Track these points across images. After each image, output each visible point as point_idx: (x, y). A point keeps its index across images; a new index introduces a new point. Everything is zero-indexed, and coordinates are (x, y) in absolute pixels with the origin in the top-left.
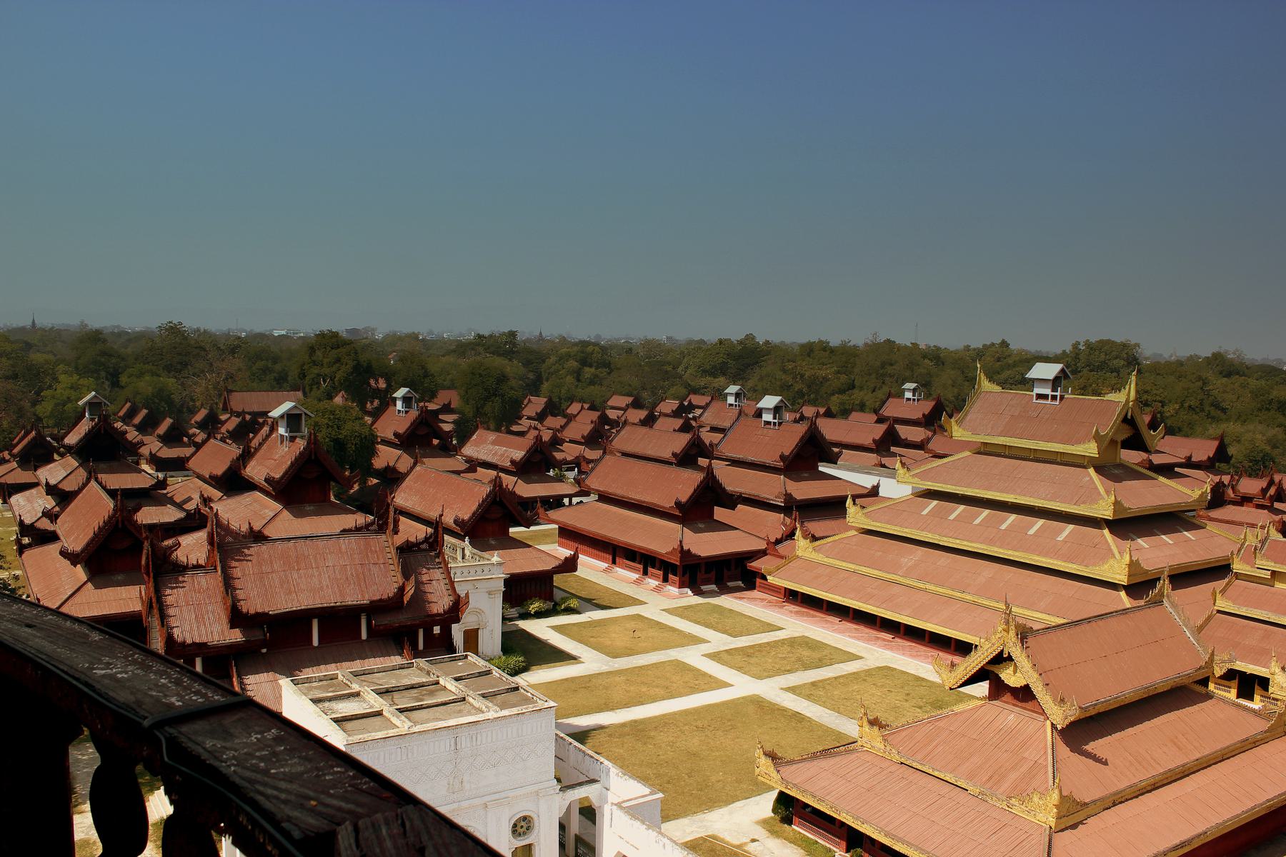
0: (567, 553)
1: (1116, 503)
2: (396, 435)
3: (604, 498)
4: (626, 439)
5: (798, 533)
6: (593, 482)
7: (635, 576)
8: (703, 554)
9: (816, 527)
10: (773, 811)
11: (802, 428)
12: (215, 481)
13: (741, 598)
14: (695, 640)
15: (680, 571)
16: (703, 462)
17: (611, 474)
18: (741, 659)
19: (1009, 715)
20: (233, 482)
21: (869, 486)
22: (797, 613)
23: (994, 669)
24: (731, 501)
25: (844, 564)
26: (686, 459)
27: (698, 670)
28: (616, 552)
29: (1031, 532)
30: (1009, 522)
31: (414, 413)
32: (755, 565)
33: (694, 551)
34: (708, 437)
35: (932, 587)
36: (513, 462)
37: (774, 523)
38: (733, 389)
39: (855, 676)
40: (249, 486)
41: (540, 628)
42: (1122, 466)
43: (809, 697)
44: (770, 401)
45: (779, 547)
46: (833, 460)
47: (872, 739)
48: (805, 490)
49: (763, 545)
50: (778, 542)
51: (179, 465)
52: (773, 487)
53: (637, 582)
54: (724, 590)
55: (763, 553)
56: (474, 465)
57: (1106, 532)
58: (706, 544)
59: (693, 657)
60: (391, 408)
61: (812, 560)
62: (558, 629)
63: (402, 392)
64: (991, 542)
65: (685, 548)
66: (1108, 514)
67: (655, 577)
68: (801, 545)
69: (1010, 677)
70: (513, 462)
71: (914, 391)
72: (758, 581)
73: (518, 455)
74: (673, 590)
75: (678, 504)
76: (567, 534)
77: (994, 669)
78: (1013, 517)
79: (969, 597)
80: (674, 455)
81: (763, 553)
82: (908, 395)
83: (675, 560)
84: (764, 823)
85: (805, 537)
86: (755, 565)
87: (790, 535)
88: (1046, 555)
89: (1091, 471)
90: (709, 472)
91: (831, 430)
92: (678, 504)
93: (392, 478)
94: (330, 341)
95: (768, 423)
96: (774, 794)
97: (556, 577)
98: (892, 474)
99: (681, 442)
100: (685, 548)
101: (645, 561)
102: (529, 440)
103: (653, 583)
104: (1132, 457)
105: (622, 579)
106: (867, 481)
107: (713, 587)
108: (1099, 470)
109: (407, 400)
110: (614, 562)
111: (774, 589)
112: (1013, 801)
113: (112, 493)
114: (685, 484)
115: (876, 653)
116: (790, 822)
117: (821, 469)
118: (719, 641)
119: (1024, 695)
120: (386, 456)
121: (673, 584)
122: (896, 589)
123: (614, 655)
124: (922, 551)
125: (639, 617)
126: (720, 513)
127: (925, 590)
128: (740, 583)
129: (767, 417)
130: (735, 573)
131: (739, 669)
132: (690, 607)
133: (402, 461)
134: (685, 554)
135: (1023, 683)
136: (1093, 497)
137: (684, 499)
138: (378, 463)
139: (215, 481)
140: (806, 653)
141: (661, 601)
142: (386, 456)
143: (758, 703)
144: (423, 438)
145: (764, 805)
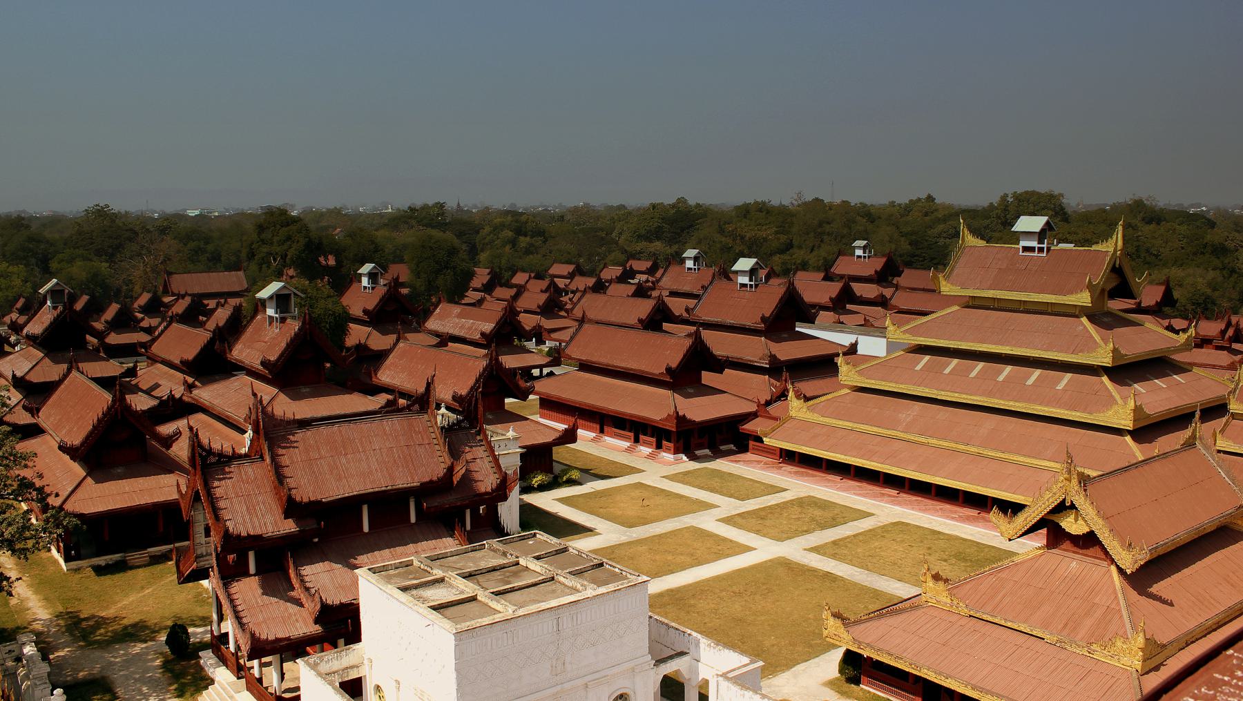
0: (562, 427)
1: (1115, 351)
3: (585, 367)
5: (791, 394)
6: (575, 352)
7: (626, 444)
8: (698, 419)
9: (808, 387)
10: (840, 671)
13: (736, 462)
14: (708, 506)
15: (674, 437)
18: (758, 521)
19: (1071, 563)
21: (847, 344)
22: (796, 473)
23: (1055, 518)
25: (841, 422)
26: (657, 320)
27: (717, 536)
28: (606, 421)
31: (381, 290)
32: (749, 427)
33: (688, 417)
36: (483, 334)
37: (762, 386)
38: (691, 253)
39: (872, 533)
41: (547, 501)
42: (1110, 314)
43: (834, 556)
45: (769, 408)
46: (810, 320)
47: (937, 594)
49: (753, 408)
50: (768, 403)
52: (756, 349)
54: (718, 454)
55: (754, 415)
56: (444, 340)
58: (700, 409)
59: (707, 522)
60: (355, 285)
61: (804, 419)
62: (563, 500)
64: (990, 394)
65: (681, 414)
68: (795, 406)
69: (1071, 525)
70: (483, 334)
71: (864, 248)
72: (751, 443)
73: (488, 327)
74: (668, 456)
77: (1055, 518)
78: (1008, 369)
80: (640, 321)
81: (754, 415)
82: (859, 252)
84: (831, 684)
85: (798, 397)
86: (749, 427)
89: (1084, 320)
96: (838, 654)
97: (554, 449)
98: (868, 327)
99: (644, 308)
101: (636, 429)
103: (646, 450)
104: (1116, 305)
106: (845, 339)
107: (707, 451)
108: (1092, 319)
110: (602, 431)
111: (769, 451)
115: (887, 510)
116: (856, 681)
118: (729, 506)
119: (1089, 541)
120: (357, 334)
121: (668, 450)
122: (897, 445)
123: (629, 524)
125: (640, 485)
127: (927, 445)
128: (732, 446)
130: (727, 437)
131: (758, 532)
132: (689, 472)
133: (378, 341)
135: (1086, 530)
136: (1091, 346)
140: (818, 513)
141: (660, 469)
143: (785, 564)
145: (830, 664)
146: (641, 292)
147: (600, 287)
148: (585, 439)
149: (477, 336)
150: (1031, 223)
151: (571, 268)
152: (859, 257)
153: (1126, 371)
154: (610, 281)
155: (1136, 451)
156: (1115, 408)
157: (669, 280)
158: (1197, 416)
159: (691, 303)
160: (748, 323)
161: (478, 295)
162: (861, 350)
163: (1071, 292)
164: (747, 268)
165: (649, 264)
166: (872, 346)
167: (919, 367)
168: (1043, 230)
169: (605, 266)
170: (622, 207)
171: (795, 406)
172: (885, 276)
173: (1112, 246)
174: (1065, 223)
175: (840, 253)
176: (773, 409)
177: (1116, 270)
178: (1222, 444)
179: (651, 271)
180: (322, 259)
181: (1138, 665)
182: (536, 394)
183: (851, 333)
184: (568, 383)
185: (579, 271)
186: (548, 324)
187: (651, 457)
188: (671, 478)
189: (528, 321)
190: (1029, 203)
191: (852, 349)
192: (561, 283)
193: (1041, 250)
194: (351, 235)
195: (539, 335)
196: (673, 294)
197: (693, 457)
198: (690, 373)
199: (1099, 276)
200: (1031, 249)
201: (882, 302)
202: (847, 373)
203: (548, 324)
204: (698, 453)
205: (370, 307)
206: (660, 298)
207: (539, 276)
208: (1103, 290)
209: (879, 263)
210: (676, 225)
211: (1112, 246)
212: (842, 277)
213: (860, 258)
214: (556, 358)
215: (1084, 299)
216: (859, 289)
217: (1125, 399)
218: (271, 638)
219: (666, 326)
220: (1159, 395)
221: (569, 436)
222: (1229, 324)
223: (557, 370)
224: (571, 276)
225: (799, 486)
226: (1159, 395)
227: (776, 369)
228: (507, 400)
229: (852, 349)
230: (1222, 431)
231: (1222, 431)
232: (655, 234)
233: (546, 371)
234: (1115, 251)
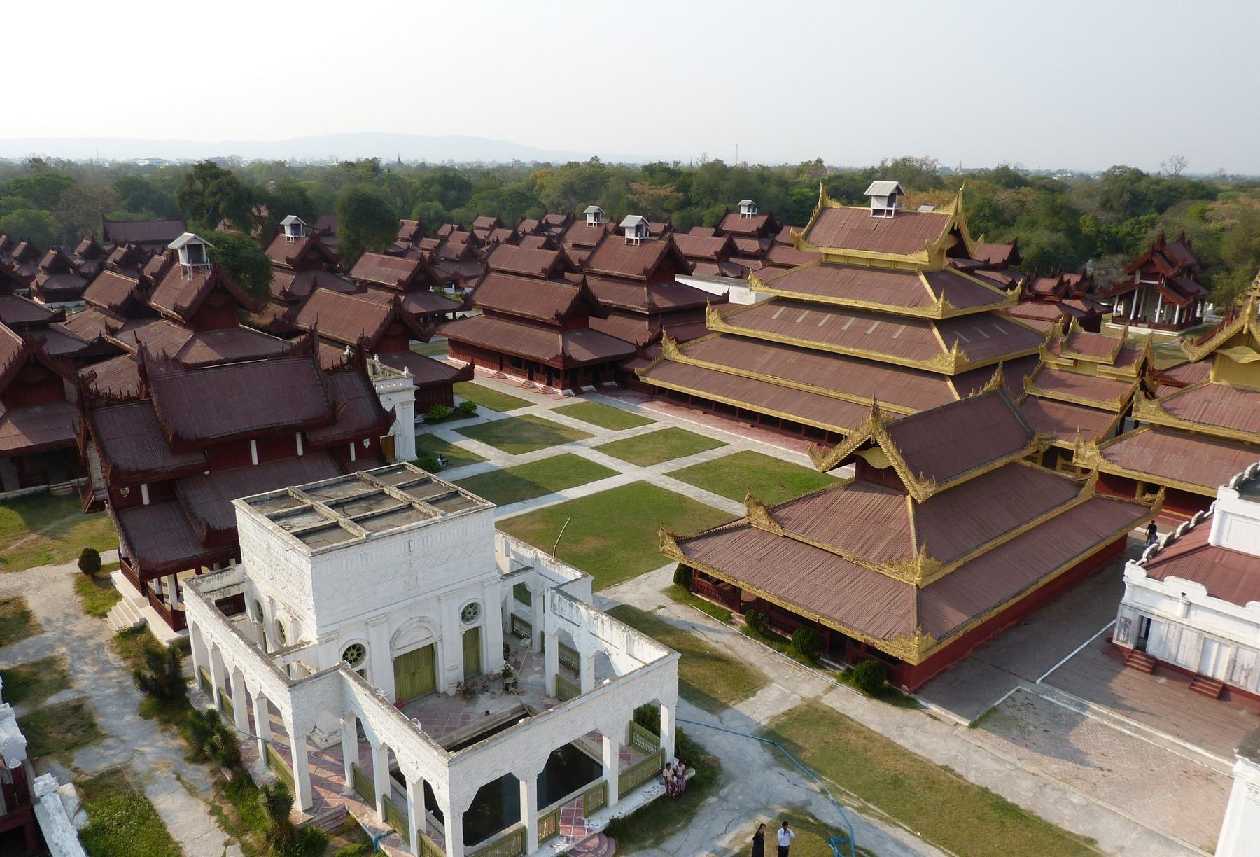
2: (288, 260)
3: (488, 312)
4: (503, 258)
6: (479, 300)
7: (522, 380)
11: (663, 244)
12: (115, 311)
16: (577, 277)
17: (494, 293)
20: (136, 310)
24: (604, 311)
26: (558, 271)
29: (870, 332)
32: (628, 366)
34: (575, 256)
35: (783, 382)
36: (400, 282)
40: (155, 315)
44: (631, 221)
49: (632, 350)
50: (646, 346)
51: (75, 294)
52: (638, 299)
53: (524, 385)
57: (935, 331)
63: (291, 218)
64: (834, 341)
67: (541, 381)
70: (400, 282)
73: (405, 275)
75: (558, 315)
76: (458, 347)
79: (816, 390)
86: (628, 366)
87: (656, 340)
88: (882, 352)
90: (584, 284)
91: (688, 244)
92: (558, 315)
93: (294, 301)
94: (209, 172)
95: (630, 241)
102: (412, 262)
105: (513, 384)
107: (591, 387)
109: (295, 227)
112: (884, 565)
113: (17, 328)
114: (563, 295)
118: (603, 435)
122: (753, 385)
124: (773, 350)
126: (594, 322)
128: (614, 383)
129: (630, 235)
134: (566, 358)
137: (563, 311)
138: (275, 290)
139: (115, 311)
140: (675, 442)
141: (545, 404)
142: (282, 281)
144: (318, 262)
146: (548, 245)
147: (515, 239)
148: (483, 374)
149: (395, 284)
151: (492, 220)
152: (744, 215)
154: (525, 234)
157: (572, 237)
160: (632, 275)
161: (404, 245)
162: (733, 299)
165: (563, 218)
166: (741, 295)
167: (775, 317)
169: (523, 220)
170: (548, 165)
172: (768, 232)
175: (728, 212)
176: (651, 352)
177: (955, 232)
180: (254, 210)
182: (444, 335)
184: (472, 324)
185: (499, 224)
186: (464, 271)
187: (543, 392)
188: (557, 410)
189: (443, 272)
191: (725, 298)
192: (480, 235)
194: (282, 188)
195: (456, 281)
196: (575, 246)
197: (579, 393)
199: (942, 239)
201: (761, 256)
203: (464, 271)
204: (584, 388)
205: (293, 255)
206: (562, 251)
207: (461, 229)
208: (941, 251)
209: (761, 221)
212: (728, 232)
213: (745, 216)
214: (468, 304)
216: (742, 244)
218: (161, 561)
219: (567, 275)
221: (467, 374)
223: (468, 314)
224: (492, 228)
227: (655, 315)
228: (412, 342)
229: (725, 298)
233: (458, 314)
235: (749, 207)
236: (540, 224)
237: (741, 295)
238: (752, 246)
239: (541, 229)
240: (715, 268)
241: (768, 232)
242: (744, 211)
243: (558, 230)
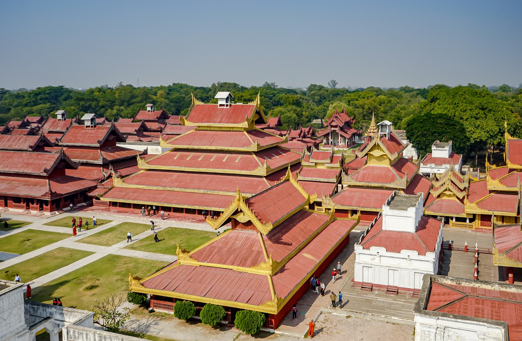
1: (258, 145)
9: (124, 171)
22: (118, 212)
26: (42, 146)
30: (214, 157)
42: (256, 131)
46: (123, 141)
48: (111, 156)
65: (53, 191)
66: (255, 149)
67: (35, 209)
72: (94, 200)
74: (47, 213)
83: (48, 198)
89: (245, 133)
99: (33, 140)
100: (53, 191)
101: (28, 202)
103: (33, 212)
108: (248, 132)
110: (6, 205)
111: (104, 203)
117: (117, 145)
121: (46, 210)
130: (83, 199)
134: (52, 194)
136: (249, 144)
146: (32, 133)
150: (222, 95)
153: (264, 153)
155: (268, 184)
156: (259, 168)
157: (47, 127)
158: (289, 167)
159: (59, 136)
162: (149, 152)
163: (240, 122)
164: (90, 118)
165: (38, 118)
168: (228, 98)
171: (117, 182)
173: (256, 103)
174: (239, 94)
177: (258, 113)
178: (300, 178)
179: (40, 122)
181: (270, 272)
183: (145, 145)
190: (223, 87)
191: (145, 152)
193: (227, 105)
196: (50, 132)
198: (60, 171)
199: (251, 115)
200: (224, 105)
202: (142, 164)
208: (253, 121)
209: (159, 113)
210: (53, 98)
211: (256, 103)
213: (149, 112)
215: (245, 125)
217: (263, 164)
219: (46, 149)
220: (278, 161)
222: (301, 132)
225: (116, 218)
226: (278, 161)
229: (145, 152)
230: (299, 173)
231: (299, 173)
232: (45, 100)
234: (257, 105)
235: (151, 107)
236: (24, 122)
237: (153, 150)
238: (154, 126)
239: (24, 125)
240: (136, 138)
241: (163, 118)
242: (149, 109)
243: (36, 125)
